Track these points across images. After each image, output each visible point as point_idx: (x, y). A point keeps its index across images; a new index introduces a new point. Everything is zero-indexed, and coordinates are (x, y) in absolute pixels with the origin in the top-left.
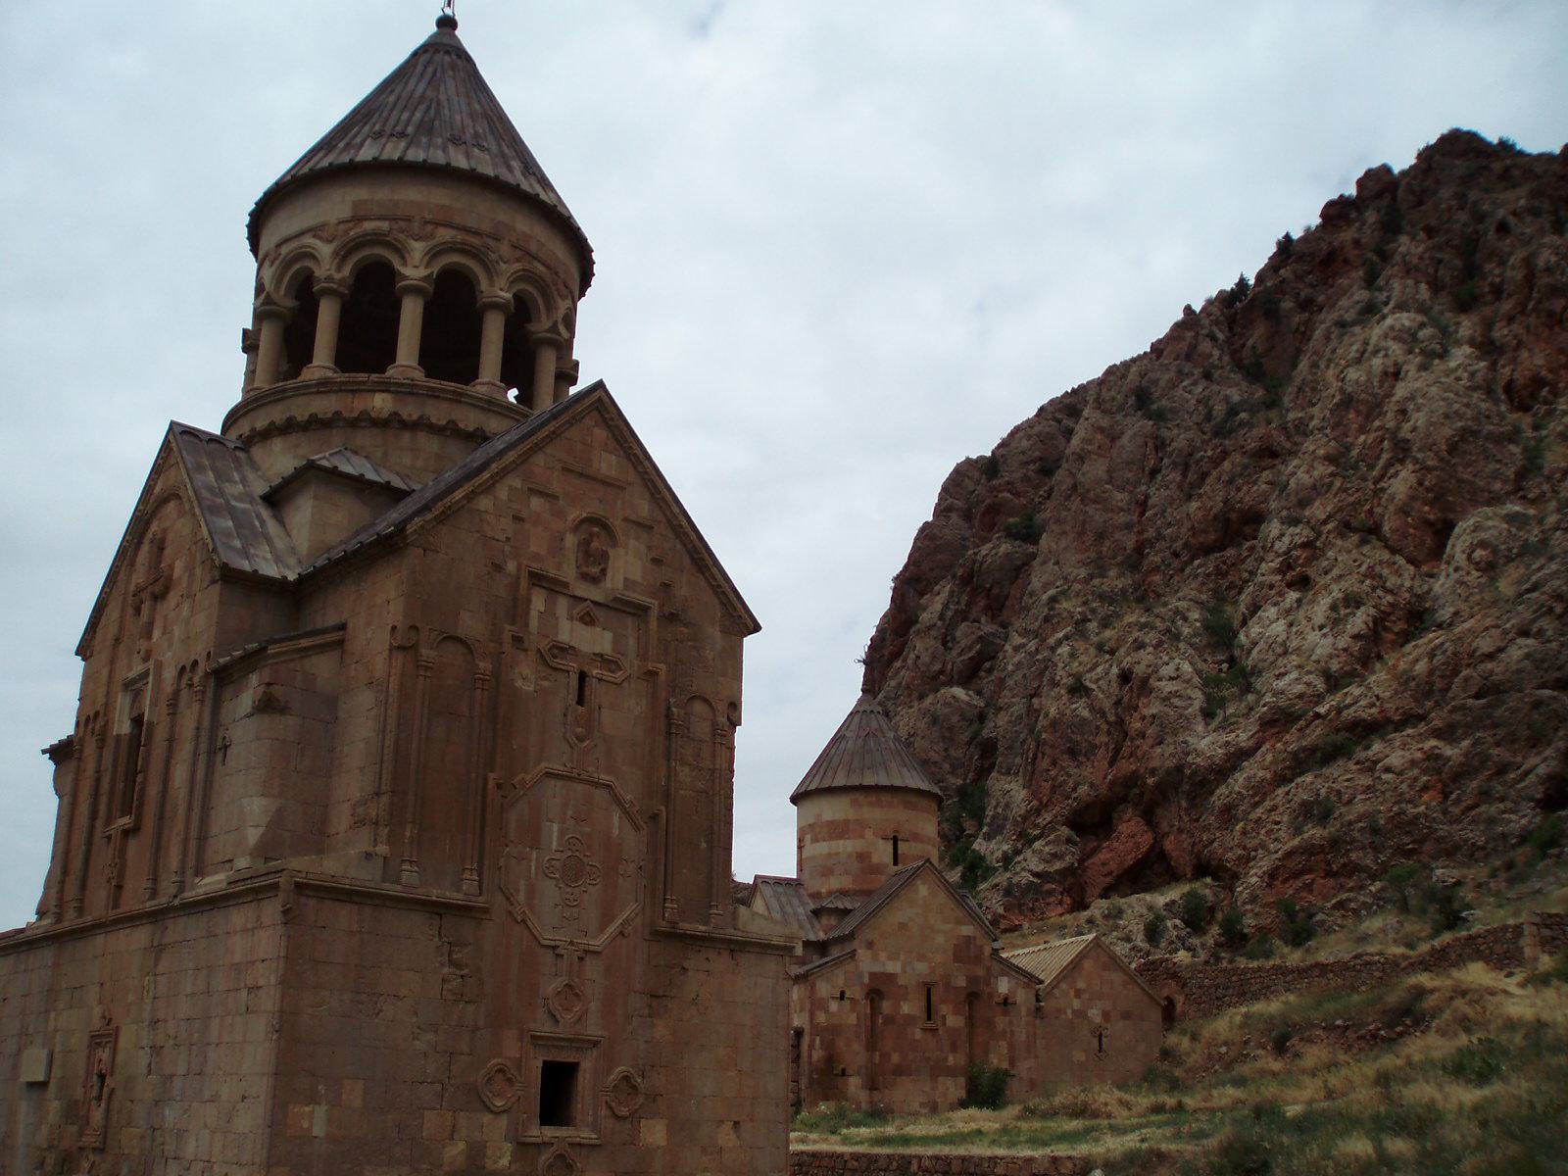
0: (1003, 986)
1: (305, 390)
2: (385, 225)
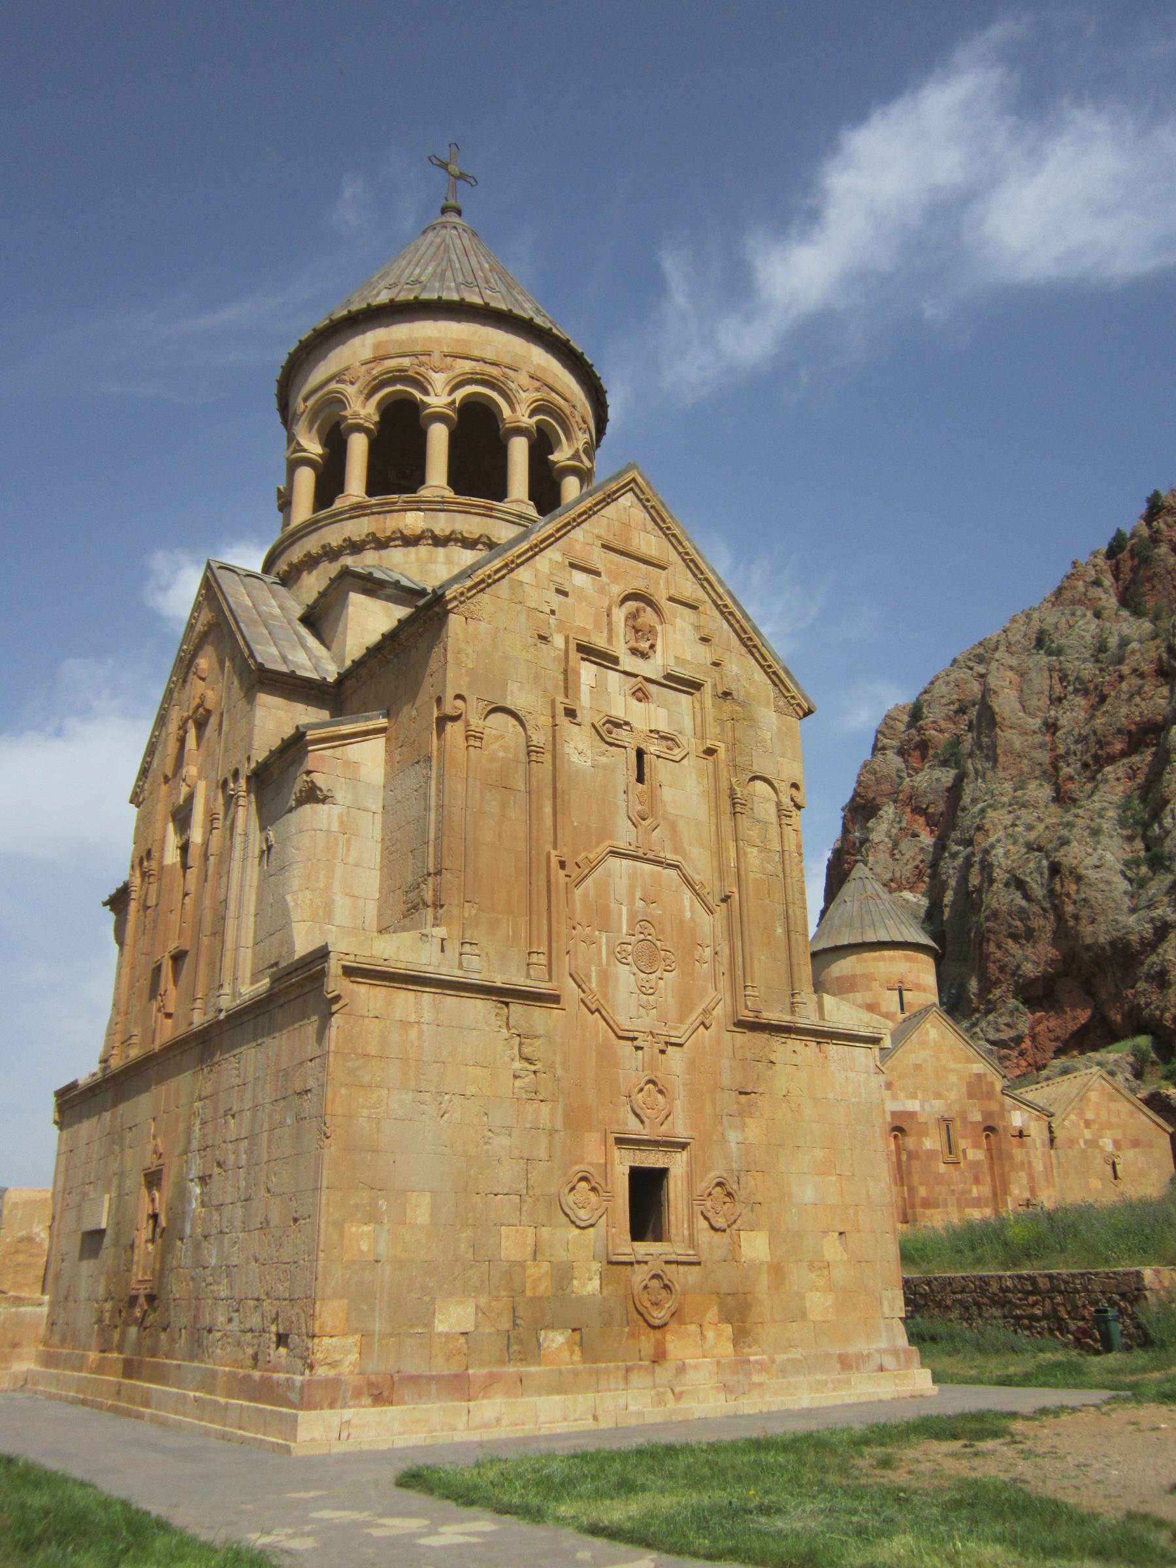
0: (1017, 1119)
1: (337, 517)
2: (406, 362)
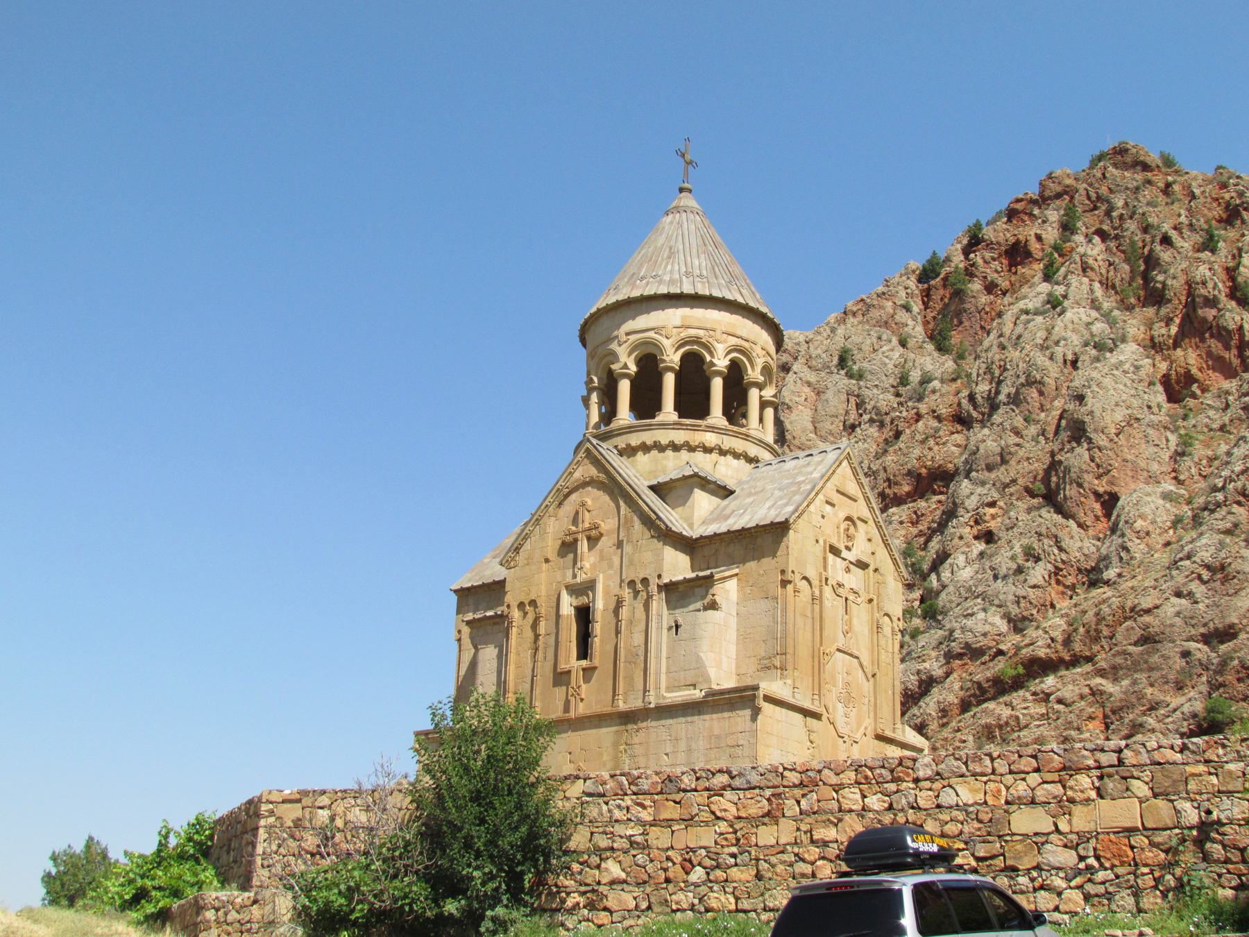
1: (664, 426)
